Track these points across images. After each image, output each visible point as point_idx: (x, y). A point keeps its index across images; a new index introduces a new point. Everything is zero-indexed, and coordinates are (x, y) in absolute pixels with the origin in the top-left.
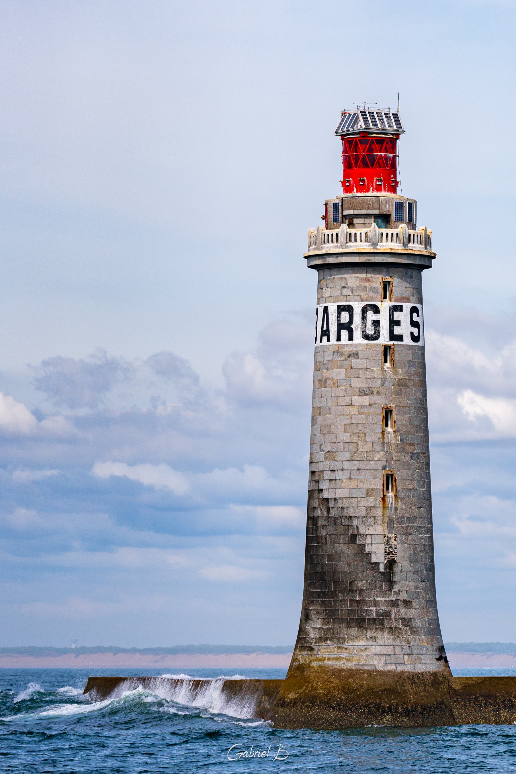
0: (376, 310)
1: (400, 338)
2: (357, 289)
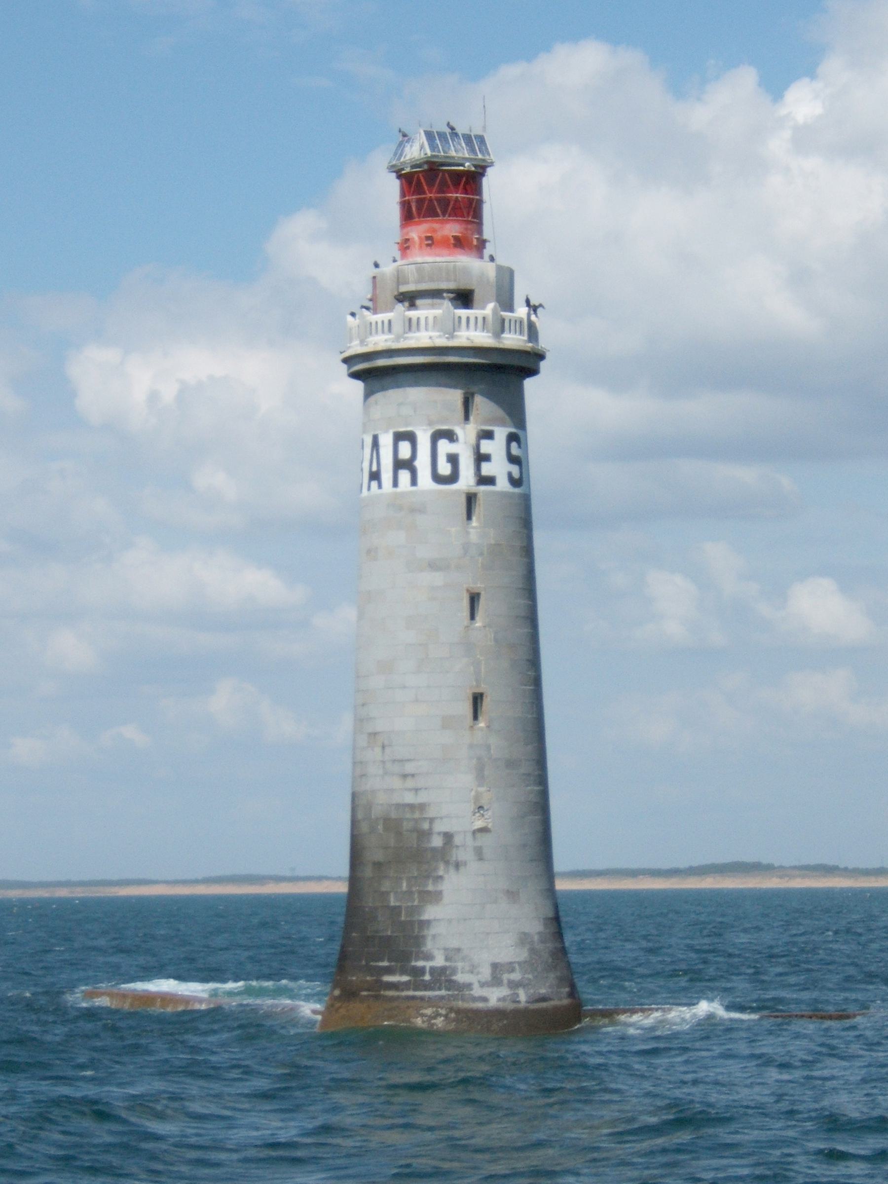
0: (450, 436)
1: (489, 481)
2: (425, 405)
